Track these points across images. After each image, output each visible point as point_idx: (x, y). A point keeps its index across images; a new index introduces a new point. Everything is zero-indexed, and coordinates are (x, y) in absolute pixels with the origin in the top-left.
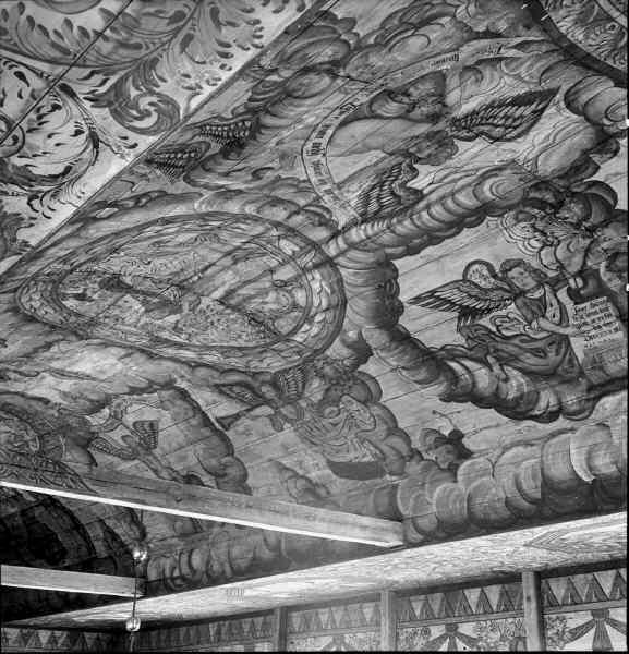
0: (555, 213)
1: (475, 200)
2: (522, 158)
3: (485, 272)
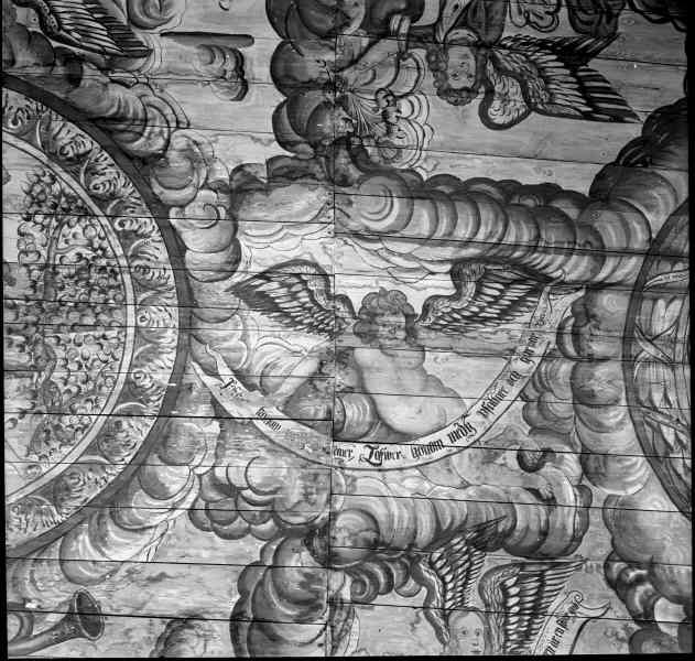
0: (354, 134)
1: (416, 213)
3: (497, 103)
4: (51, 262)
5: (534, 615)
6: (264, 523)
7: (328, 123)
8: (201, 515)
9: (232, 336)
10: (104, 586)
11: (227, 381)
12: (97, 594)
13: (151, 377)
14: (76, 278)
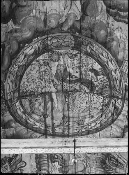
5: (118, 161)
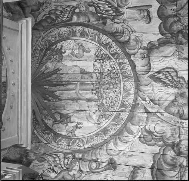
0: (183, 29)
2: (176, 59)
4: (101, 72)
6: (160, 142)
7: (175, 27)
8: (142, 139)
9: (149, 90)
10: (117, 157)
11: (148, 102)
12: (115, 158)
13: (128, 101)
14: (108, 76)
